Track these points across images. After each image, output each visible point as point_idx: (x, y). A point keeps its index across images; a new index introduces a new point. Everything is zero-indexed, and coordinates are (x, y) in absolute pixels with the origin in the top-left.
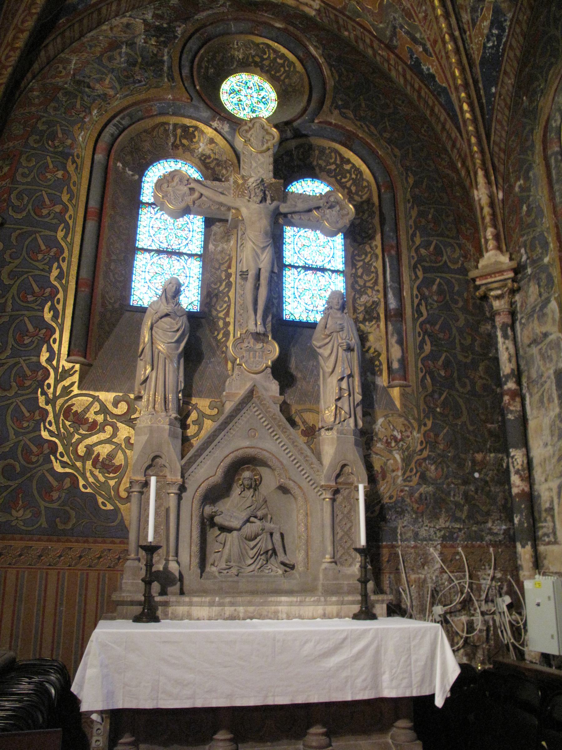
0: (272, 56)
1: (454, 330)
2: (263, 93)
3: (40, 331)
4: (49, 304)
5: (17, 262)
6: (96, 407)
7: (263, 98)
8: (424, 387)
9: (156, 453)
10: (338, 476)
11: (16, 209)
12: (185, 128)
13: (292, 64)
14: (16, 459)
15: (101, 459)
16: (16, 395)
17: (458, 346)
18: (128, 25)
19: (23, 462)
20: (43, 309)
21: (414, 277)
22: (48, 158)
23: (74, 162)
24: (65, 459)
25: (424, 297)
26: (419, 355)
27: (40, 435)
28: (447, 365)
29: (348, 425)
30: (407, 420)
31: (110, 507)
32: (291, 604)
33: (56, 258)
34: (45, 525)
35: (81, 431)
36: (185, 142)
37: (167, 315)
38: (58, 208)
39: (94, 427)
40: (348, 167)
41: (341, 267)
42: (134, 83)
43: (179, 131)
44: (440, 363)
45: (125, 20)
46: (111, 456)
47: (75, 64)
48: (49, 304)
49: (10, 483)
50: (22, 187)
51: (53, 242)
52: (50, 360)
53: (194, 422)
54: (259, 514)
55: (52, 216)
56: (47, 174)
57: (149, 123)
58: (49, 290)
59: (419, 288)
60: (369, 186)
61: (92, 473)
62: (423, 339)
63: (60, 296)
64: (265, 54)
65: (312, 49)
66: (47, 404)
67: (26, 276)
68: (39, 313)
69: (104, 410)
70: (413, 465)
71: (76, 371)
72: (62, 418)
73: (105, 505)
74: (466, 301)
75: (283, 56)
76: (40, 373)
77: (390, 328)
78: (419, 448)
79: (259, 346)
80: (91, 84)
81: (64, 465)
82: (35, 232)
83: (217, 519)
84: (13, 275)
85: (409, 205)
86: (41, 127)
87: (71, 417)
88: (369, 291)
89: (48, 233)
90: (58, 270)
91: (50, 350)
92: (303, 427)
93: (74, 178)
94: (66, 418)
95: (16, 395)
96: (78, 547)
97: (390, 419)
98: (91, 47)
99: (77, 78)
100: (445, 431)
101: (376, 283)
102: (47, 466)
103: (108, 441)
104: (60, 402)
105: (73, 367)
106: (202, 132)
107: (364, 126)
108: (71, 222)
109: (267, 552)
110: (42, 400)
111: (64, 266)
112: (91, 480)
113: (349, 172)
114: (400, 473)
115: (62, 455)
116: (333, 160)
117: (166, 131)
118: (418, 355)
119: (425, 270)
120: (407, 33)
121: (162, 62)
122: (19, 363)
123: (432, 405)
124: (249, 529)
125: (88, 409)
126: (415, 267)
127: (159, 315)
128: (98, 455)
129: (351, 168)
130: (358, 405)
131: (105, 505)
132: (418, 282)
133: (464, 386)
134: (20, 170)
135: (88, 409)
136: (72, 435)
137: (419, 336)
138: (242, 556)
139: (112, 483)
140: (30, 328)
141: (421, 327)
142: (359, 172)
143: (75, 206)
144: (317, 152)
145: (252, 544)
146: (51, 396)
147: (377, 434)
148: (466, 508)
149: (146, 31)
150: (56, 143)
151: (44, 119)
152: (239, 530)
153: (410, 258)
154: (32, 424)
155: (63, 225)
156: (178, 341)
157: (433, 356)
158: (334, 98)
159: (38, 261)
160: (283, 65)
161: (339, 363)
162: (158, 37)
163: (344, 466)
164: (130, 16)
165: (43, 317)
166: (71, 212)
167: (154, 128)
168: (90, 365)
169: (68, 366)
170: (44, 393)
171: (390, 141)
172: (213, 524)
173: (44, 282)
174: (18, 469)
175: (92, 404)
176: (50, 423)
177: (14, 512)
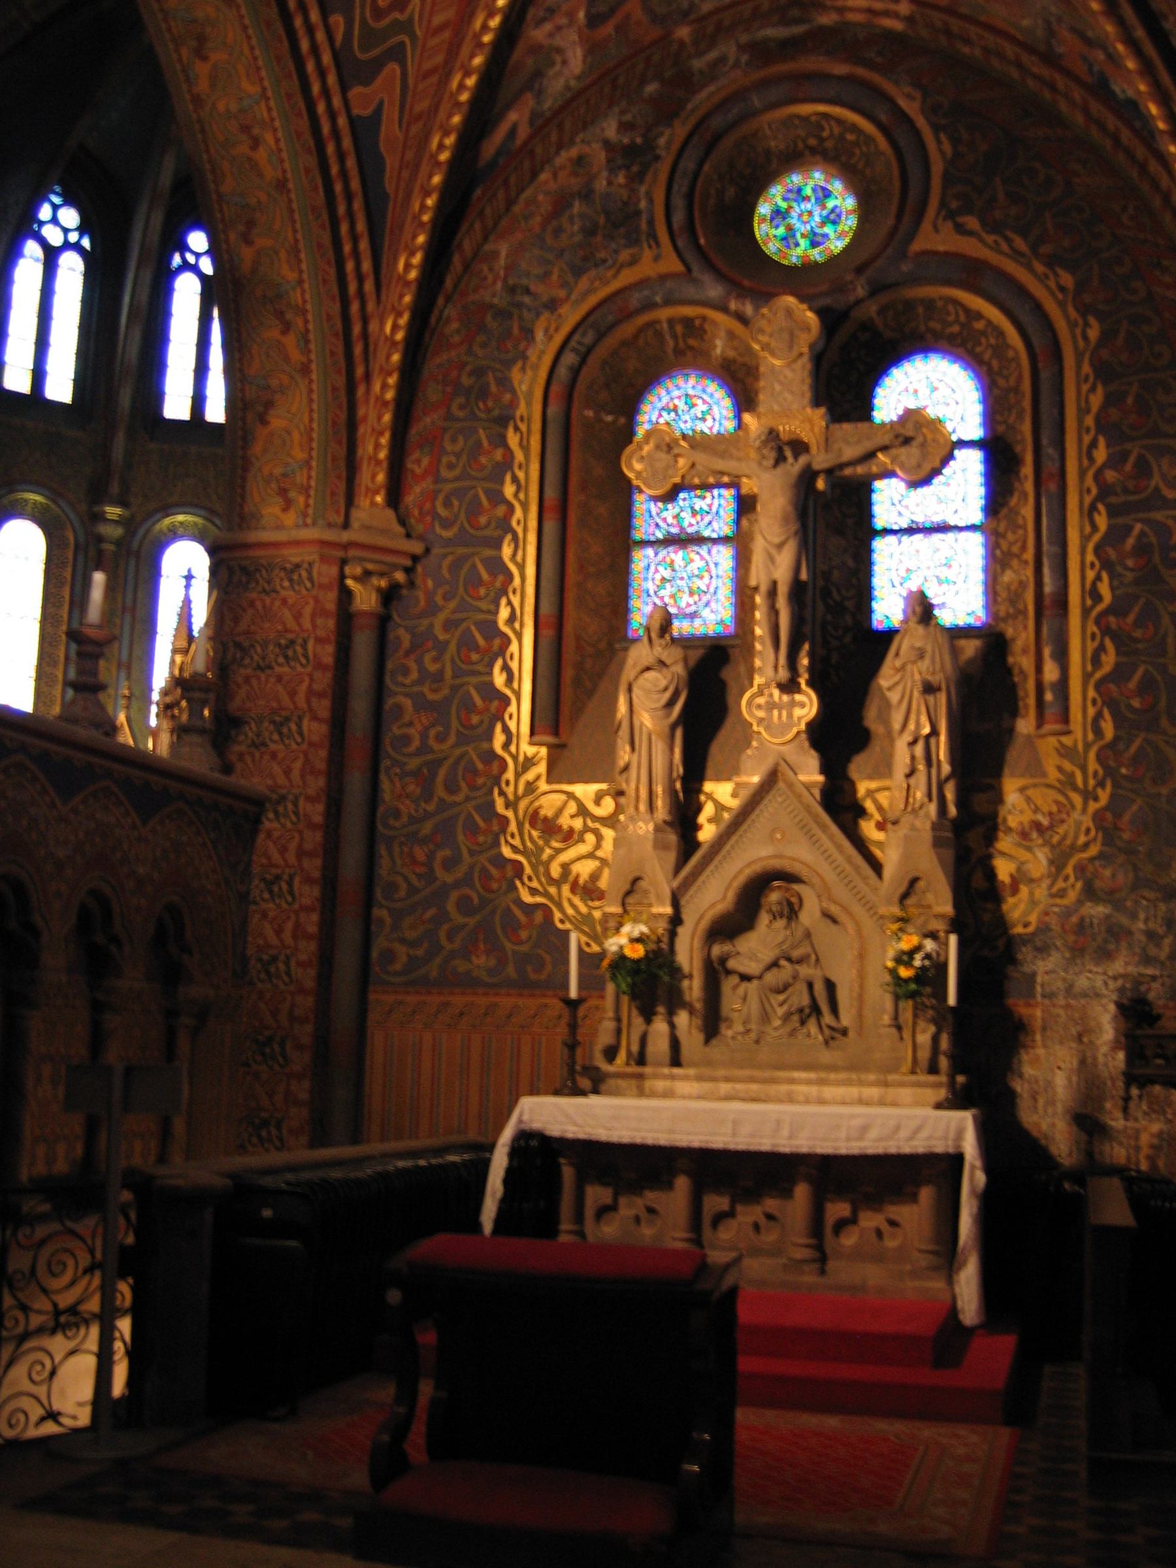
0: (837, 130)
2: (830, 204)
5: (452, 605)
6: (572, 808)
7: (833, 211)
8: (1098, 732)
9: (637, 874)
10: (905, 896)
11: (447, 524)
12: (688, 322)
13: (869, 139)
14: (472, 886)
15: (581, 881)
16: (468, 799)
18: (580, 161)
19: (481, 890)
21: (1088, 529)
22: (481, 431)
23: (517, 429)
24: (535, 884)
25: (1106, 565)
26: (1090, 675)
27: (501, 855)
28: (1147, 686)
29: (927, 815)
30: (1060, 791)
32: (809, 1082)
36: (692, 342)
37: (648, 669)
38: (501, 510)
39: (570, 837)
40: (979, 325)
41: (977, 517)
42: (596, 265)
43: (679, 329)
44: (1132, 685)
45: (574, 152)
46: (595, 877)
47: (507, 256)
50: (449, 487)
51: (498, 567)
52: (506, 746)
53: (710, 821)
54: (795, 954)
55: (493, 525)
57: (628, 329)
59: (1098, 550)
60: (1016, 359)
61: (569, 900)
63: (514, 647)
64: (823, 129)
65: (902, 102)
66: (507, 807)
67: (465, 624)
68: (485, 678)
69: (583, 811)
70: (1069, 870)
72: (527, 826)
75: (854, 128)
77: (1045, 629)
78: (1082, 839)
79: (785, 698)
80: (532, 288)
81: (533, 892)
82: (473, 554)
83: (732, 964)
84: (449, 625)
85: (1085, 388)
86: (466, 381)
87: (540, 825)
88: (1015, 563)
89: (488, 552)
92: (878, 817)
93: (519, 456)
94: (533, 824)
97: (1030, 792)
98: (526, 218)
99: (511, 282)
100: (1135, 808)
101: (1024, 548)
102: (511, 896)
103: (591, 856)
104: (522, 805)
105: (538, 753)
106: (714, 323)
108: (520, 530)
109: (801, 1010)
110: (499, 803)
111: (516, 601)
113: (984, 333)
114: (1045, 883)
115: (530, 879)
116: (951, 318)
117: (659, 334)
118: (1086, 677)
119: (1113, 512)
120: (1072, 29)
121: (638, 213)
122: (466, 753)
124: (771, 978)
125: (560, 811)
126: (1093, 508)
127: (639, 668)
128: (578, 876)
129: (987, 326)
130: (947, 779)
132: (1097, 537)
134: (445, 460)
135: (560, 811)
136: (542, 850)
138: (765, 1018)
140: (479, 702)
142: (1001, 334)
143: (525, 506)
144: (920, 310)
145: (781, 997)
147: (1005, 820)
148: (1167, 941)
149: (609, 161)
150: (490, 404)
151: (468, 368)
153: (1083, 491)
154: (490, 839)
156: (670, 704)
157: (1119, 674)
158: (944, 195)
159: (480, 599)
160: (857, 144)
161: (913, 717)
162: (627, 168)
163: (914, 881)
164: (583, 141)
166: (518, 513)
167: (636, 336)
168: (562, 746)
169: (530, 750)
170: (502, 793)
172: (729, 972)
173: (490, 629)
174: (476, 901)
175: (565, 804)
176: (513, 836)
177: (474, 958)
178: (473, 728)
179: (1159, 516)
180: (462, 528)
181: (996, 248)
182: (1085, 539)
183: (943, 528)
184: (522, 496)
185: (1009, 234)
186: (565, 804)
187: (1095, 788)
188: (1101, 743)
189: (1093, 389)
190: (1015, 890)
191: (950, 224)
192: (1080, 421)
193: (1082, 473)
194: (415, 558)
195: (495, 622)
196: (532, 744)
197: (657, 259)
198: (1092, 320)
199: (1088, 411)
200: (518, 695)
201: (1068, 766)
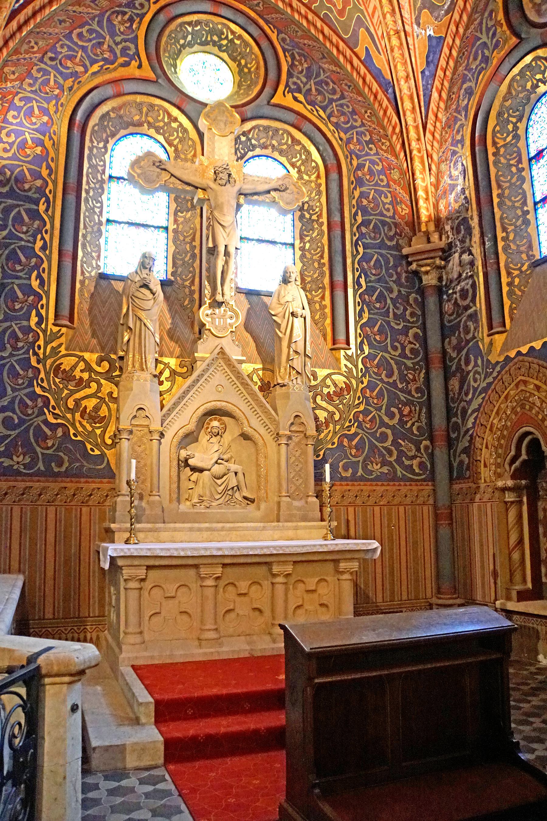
0: (230, 37)
1: (389, 301)
3: (28, 297)
4: (36, 272)
6: (82, 365)
8: (362, 350)
15: (88, 411)
16: (11, 355)
17: (391, 315)
21: (355, 253)
22: (27, 134)
24: (57, 411)
27: (34, 391)
31: (97, 452)
33: (39, 231)
34: (42, 468)
35: (70, 387)
39: (81, 384)
46: (97, 409)
48: (35, 273)
49: (9, 432)
51: (34, 215)
52: (39, 324)
54: (225, 457)
55: (33, 190)
56: (26, 150)
58: (34, 260)
61: (80, 423)
62: (362, 307)
63: (45, 265)
66: (38, 362)
67: (13, 246)
69: (88, 368)
72: (52, 375)
73: (93, 451)
74: (399, 275)
76: (30, 336)
78: (357, 402)
81: (56, 416)
83: (191, 462)
87: (60, 375)
90: (42, 241)
91: (39, 315)
93: (52, 154)
95: (11, 355)
96: (71, 486)
104: (49, 362)
105: (60, 330)
108: (51, 196)
109: (233, 488)
111: (47, 237)
112: (80, 429)
118: (356, 322)
119: (365, 247)
122: (11, 326)
123: (369, 366)
124: (217, 469)
131: (93, 451)
132: (359, 257)
133: (395, 348)
137: (359, 305)
139: (98, 432)
141: (360, 296)
146: (41, 356)
152: (209, 470)
153: (353, 234)
155: (44, 199)
157: (370, 323)
165: (31, 284)
166: (51, 186)
169: (55, 329)
170: (35, 354)
171: (337, 125)
173: (30, 252)
174: (16, 421)
175: (77, 364)
177: (15, 458)
178: (15, 310)
179: (384, 252)
180: (12, 187)
181: (311, 112)
182: (354, 257)
183: (273, 243)
184: (53, 177)
186: (77, 364)
187: (361, 377)
188: (364, 355)
190: (327, 426)
191: (290, 94)
192: (350, 202)
193: (352, 225)
195: (33, 248)
196: (55, 325)
197: (140, 66)
201: (350, 366)
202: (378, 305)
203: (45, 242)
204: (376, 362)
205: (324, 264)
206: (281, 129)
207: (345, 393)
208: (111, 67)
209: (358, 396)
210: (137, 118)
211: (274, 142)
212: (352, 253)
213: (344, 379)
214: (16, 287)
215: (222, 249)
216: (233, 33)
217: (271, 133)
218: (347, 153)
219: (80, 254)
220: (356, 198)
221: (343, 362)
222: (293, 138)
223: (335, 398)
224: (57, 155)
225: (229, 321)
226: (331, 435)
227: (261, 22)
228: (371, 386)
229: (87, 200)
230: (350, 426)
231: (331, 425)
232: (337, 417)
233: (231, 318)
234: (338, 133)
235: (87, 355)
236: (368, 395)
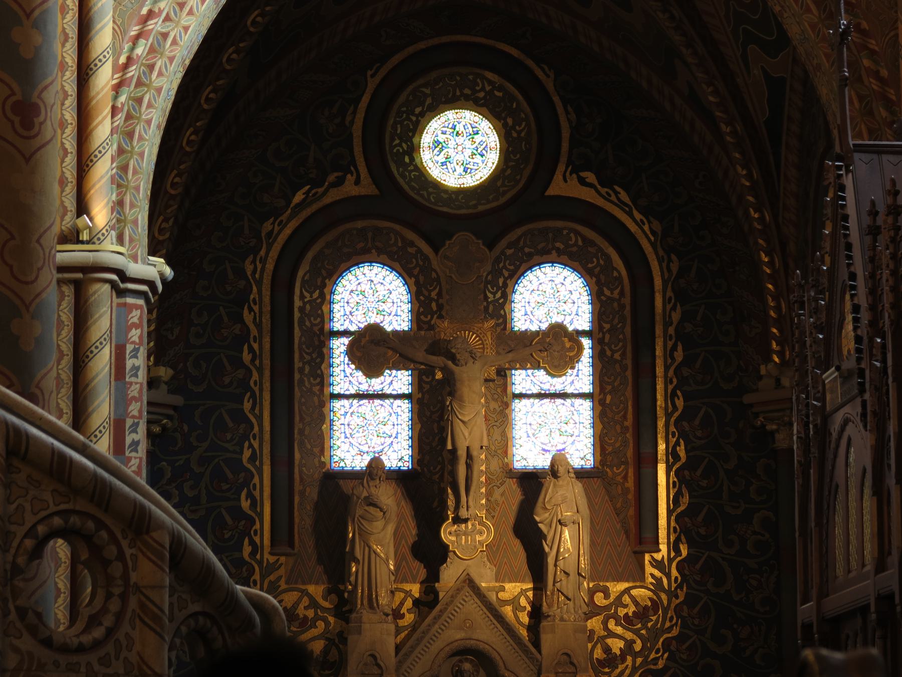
6: (305, 601)
8: (678, 552)
20: (240, 496)
22: (221, 308)
23: (251, 310)
25: (683, 435)
26: (674, 510)
33: (245, 437)
51: (240, 417)
52: (253, 554)
53: (409, 611)
63: (256, 480)
67: (216, 460)
69: (314, 604)
71: (282, 564)
76: (244, 569)
78: (668, 624)
85: (669, 307)
91: (252, 543)
93: (254, 331)
105: (278, 560)
107: (611, 192)
108: (256, 389)
111: (256, 445)
118: (670, 512)
123: (687, 572)
126: (674, 395)
132: (676, 415)
143: (260, 370)
155: (248, 394)
166: (255, 376)
169: (272, 559)
175: (299, 600)
182: (668, 416)
184: (257, 362)
185: (616, 188)
186: (299, 600)
187: (676, 588)
188: (679, 559)
189: (674, 308)
190: (623, 660)
191: (574, 176)
192: (665, 331)
193: (667, 368)
194: (175, 408)
195: (241, 461)
196: (271, 554)
197: (357, 182)
198: (674, 257)
199: (671, 324)
200: (261, 516)
201: (657, 573)
202: (704, 483)
203: (254, 451)
204: (698, 566)
205: (627, 428)
206: (565, 228)
207: (651, 612)
208: (321, 190)
209: (669, 615)
210: (362, 245)
211: (558, 245)
212: (666, 408)
213: (649, 593)
214: (224, 512)
215: (462, 453)
216: (490, 82)
217: (551, 235)
218: (661, 253)
219: (297, 455)
220: (675, 322)
221: (649, 569)
222: (584, 239)
223: (635, 621)
224: (260, 331)
225: (478, 538)
226: (628, 672)
227: (530, 63)
228: (690, 601)
229: (301, 381)
230: (657, 659)
231: (629, 658)
232: (638, 646)
233: (481, 533)
234: (649, 222)
235: (311, 589)
236: (685, 614)
